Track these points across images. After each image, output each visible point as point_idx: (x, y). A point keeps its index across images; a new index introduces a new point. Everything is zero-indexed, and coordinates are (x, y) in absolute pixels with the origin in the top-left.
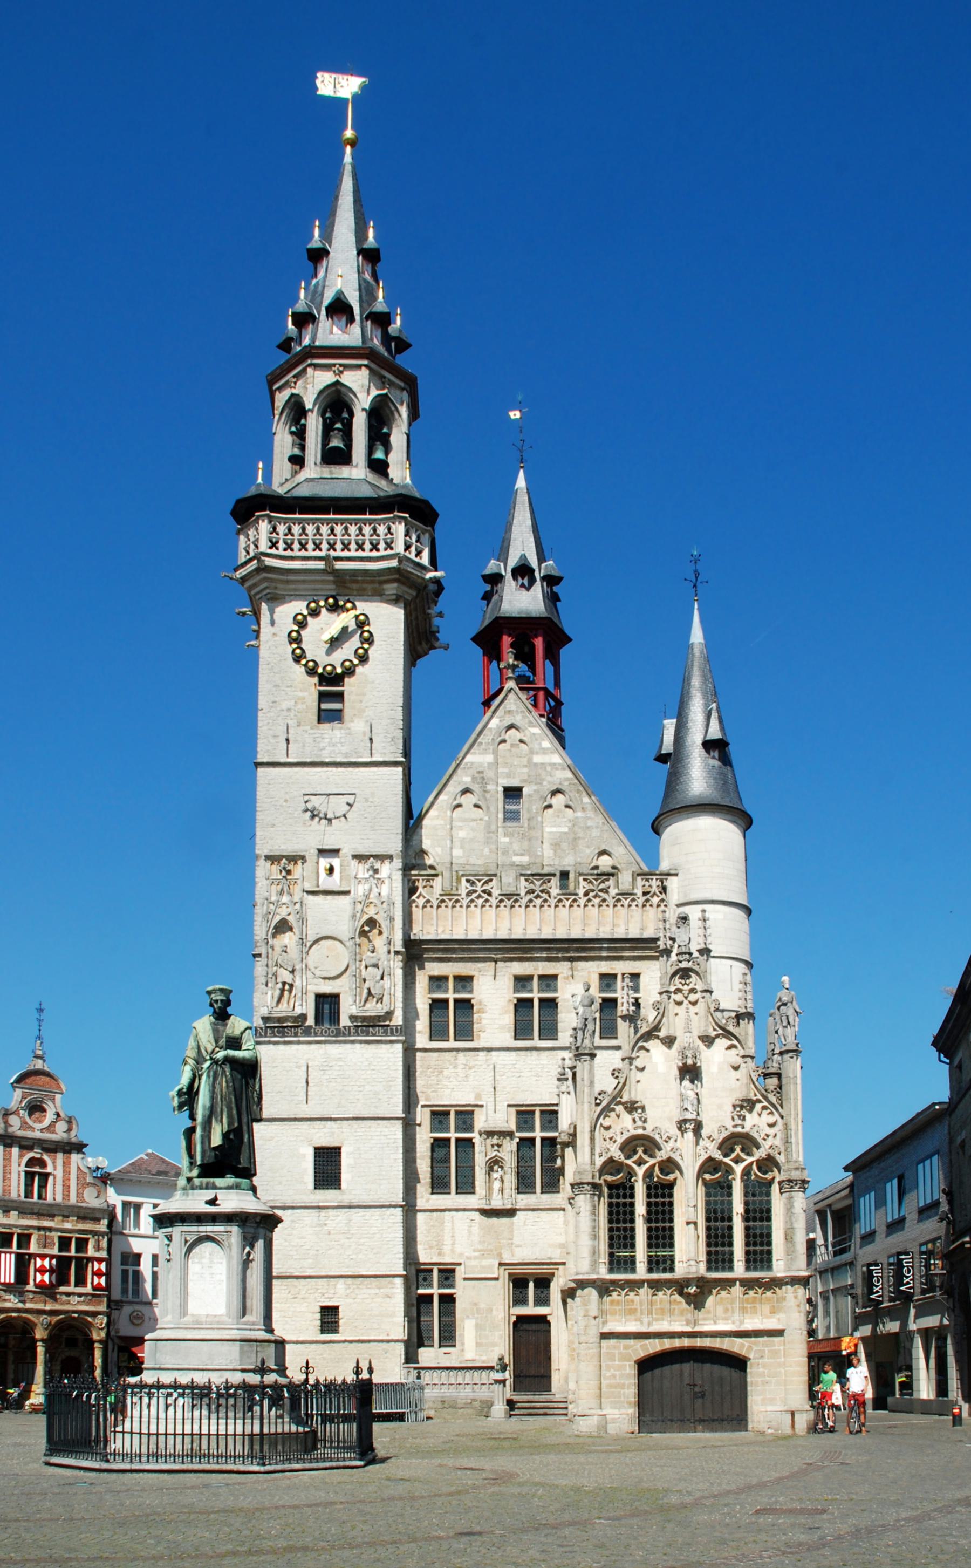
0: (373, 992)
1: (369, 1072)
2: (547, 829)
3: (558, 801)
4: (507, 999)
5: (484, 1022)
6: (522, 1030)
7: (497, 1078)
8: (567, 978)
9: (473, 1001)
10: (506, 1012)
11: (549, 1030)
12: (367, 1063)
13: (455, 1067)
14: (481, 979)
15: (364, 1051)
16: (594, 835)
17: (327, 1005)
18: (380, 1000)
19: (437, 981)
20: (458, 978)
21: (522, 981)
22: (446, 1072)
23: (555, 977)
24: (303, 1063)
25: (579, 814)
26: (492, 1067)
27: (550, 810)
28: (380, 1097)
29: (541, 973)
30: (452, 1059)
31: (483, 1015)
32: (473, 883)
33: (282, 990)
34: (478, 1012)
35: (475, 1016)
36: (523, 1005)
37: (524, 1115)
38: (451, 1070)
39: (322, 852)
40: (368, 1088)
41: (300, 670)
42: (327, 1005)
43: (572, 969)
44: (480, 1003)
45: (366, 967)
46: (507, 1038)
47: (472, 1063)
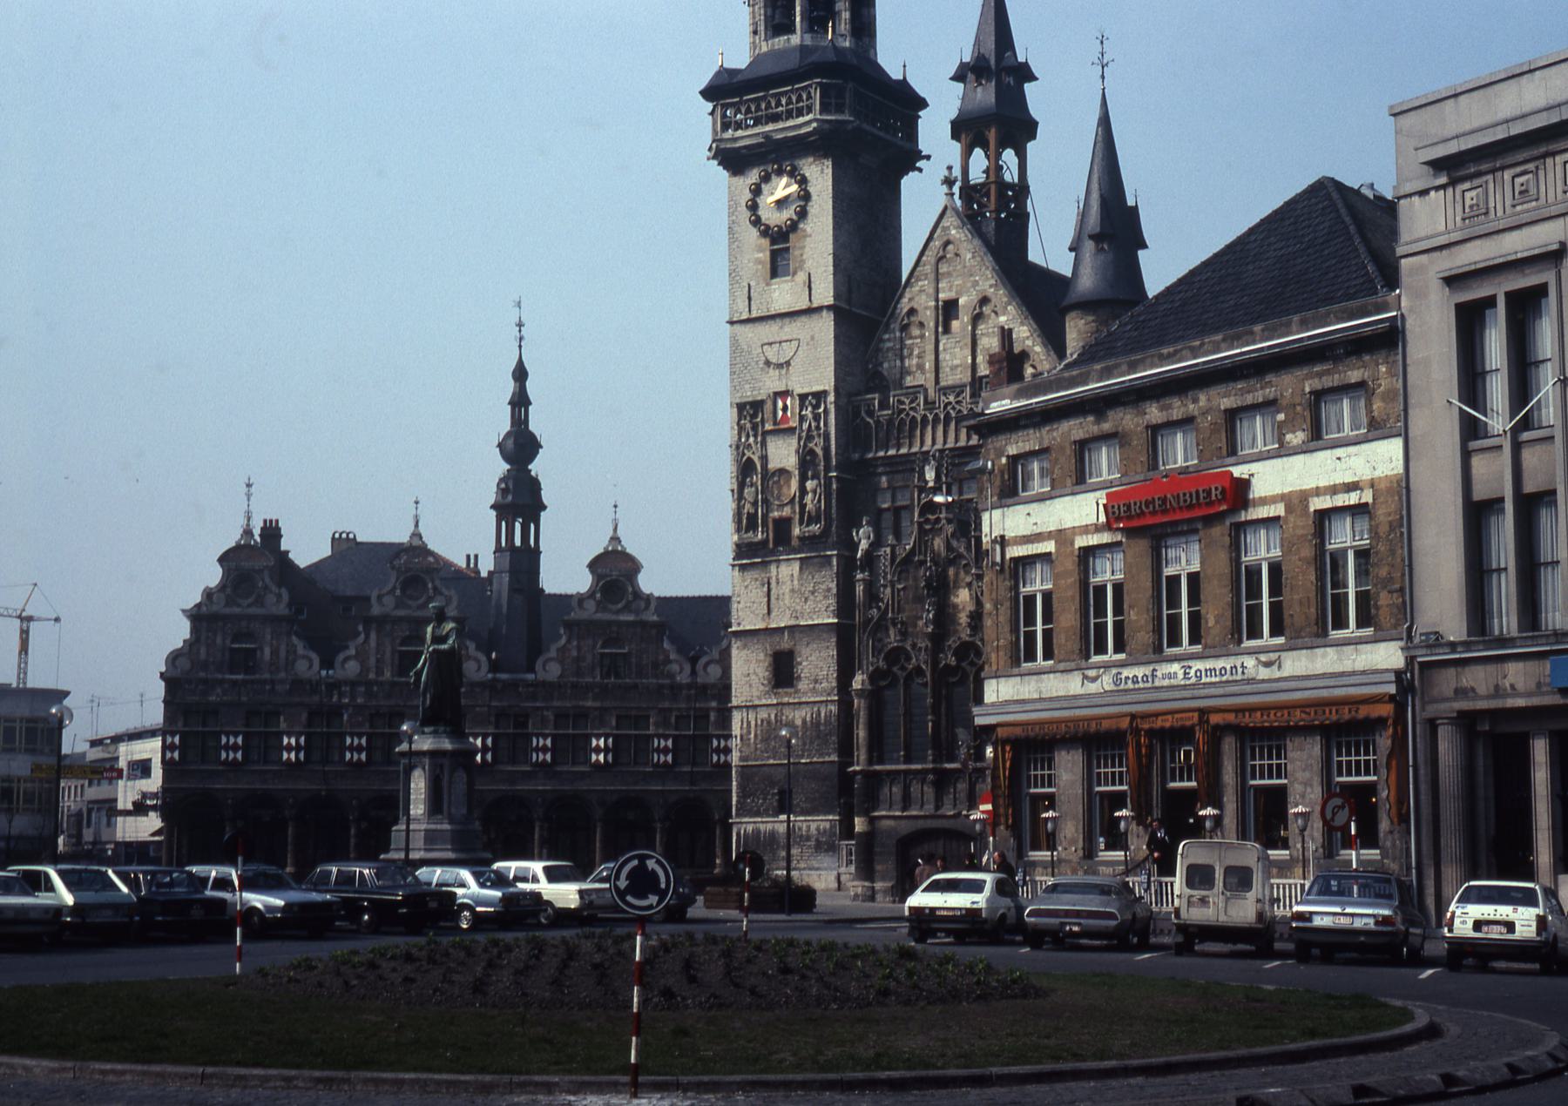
3: (986, 310)
39: (777, 394)
41: (754, 232)
42: (783, 526)
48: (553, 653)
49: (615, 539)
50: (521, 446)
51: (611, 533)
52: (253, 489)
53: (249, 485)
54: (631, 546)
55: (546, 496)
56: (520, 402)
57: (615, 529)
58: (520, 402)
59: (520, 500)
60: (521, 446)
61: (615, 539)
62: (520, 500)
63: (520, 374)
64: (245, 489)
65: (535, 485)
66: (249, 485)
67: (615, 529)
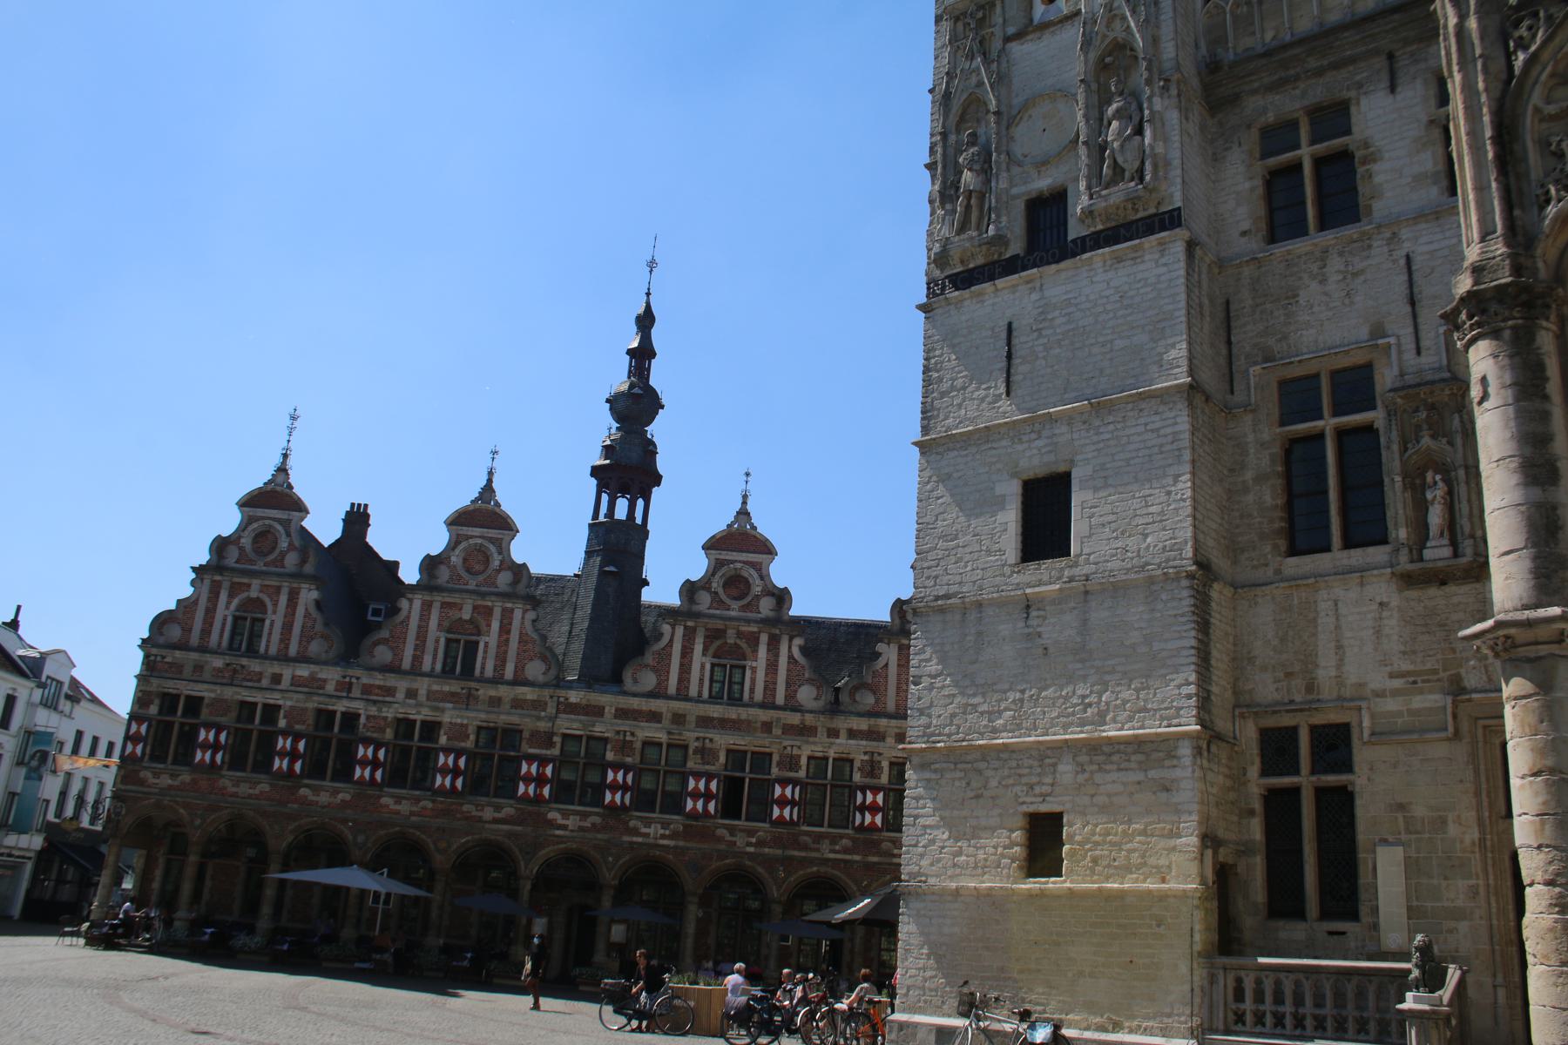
0: (1120, 160)
4: (1424, 119)
5: (1377, 179)
13: (1323, 281)
14: (1364, 102)
15: (1111, 274)
17: (1046, 211)
18: (1140, 175)
19: (1277, 136)
24: (1003, 324)
26: (1403, 262)
31: (1375, 167)
33: (968, 208)
34: (1365, 161)
35: (1361, 170)
38: (1314, 285)
42: (1046, 211)
44: (1366, 145)
48: (649, 658)
49: (743, 513)
50: (636, 406)
51: (738, 506)
52: (296, 424)
53: (294, 418)
54: (764, 525)
55: (662, 464)
56: (642, 356)
57: (744, 503)
58: (642, 356)
59: (629, 469)
60: (636, 406)
61: (743, 513)
62: (629, 469)
63: (646, 321)
64: (289, 422)
65: (650, 449)
66: (294, 418)
67: (744, 503)
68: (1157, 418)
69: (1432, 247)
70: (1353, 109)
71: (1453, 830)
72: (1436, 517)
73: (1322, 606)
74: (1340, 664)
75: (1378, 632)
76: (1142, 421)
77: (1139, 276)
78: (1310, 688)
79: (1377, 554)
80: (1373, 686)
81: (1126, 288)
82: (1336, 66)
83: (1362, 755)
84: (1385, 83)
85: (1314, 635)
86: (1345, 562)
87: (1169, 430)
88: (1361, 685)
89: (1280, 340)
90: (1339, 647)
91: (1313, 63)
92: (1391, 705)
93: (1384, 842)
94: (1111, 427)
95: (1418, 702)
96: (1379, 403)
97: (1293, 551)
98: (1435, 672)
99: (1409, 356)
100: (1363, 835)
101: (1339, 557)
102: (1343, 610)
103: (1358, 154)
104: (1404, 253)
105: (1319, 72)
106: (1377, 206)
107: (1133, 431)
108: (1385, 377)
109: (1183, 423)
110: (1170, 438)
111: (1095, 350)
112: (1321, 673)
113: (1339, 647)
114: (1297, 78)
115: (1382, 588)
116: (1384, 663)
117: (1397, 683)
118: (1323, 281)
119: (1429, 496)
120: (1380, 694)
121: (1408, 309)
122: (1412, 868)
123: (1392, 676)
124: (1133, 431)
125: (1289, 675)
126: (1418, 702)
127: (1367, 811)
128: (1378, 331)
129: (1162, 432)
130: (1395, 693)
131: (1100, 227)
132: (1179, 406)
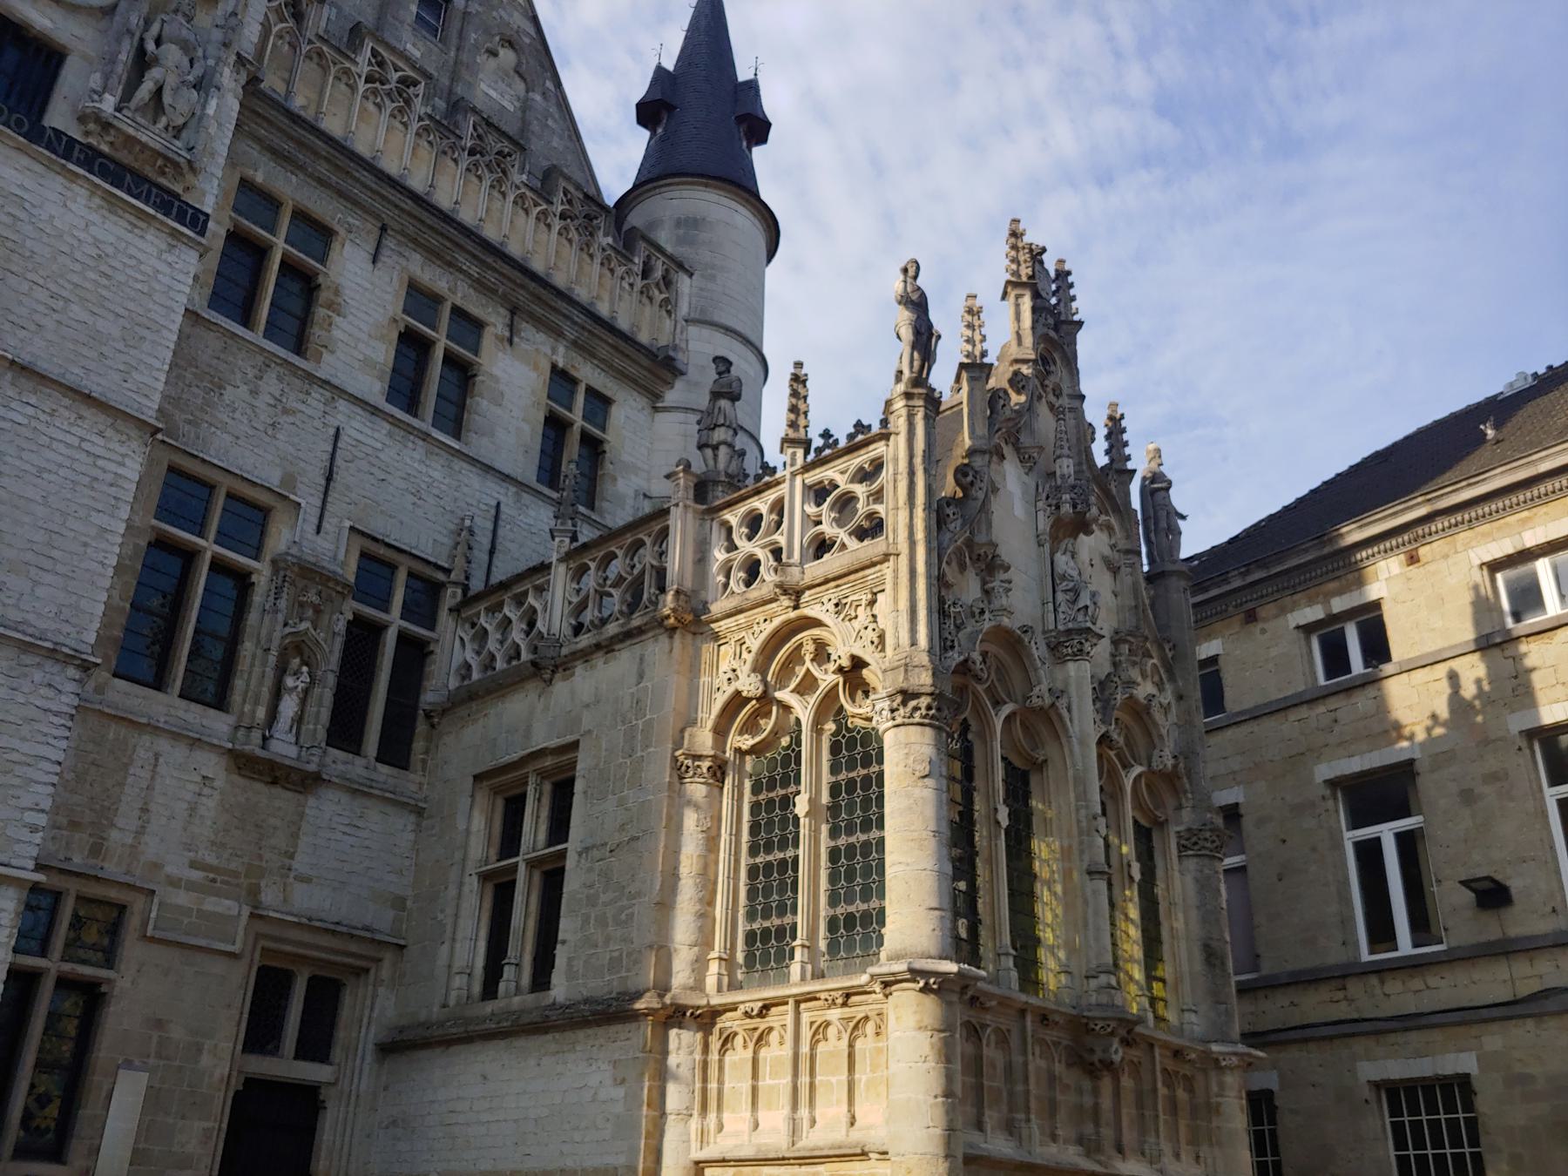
0: (167, 98)
1: (92, 275)
2: (483, 86)
3: (507, 56)
5: (336, 333)
6: (405, 389)
7: (339, 461)
8: (500, 339)
9: (321, 279)
10: (382, 338)
11: (454, 418)
12: (94, 252)
13: (254, 392)
15: (94, 217)
16: (555, 144)
20: (300, 216)
21: (420, 298)
22: (229, 393)
23: (478, 325)
25: (538, 98)
26: (332, 431)
27: (492, 63)
28: (104, 349)
29: (459, 303)
30: (251, 373)
31: (337, 319)
32: (381, 64)
34: (330, 306)
35: (320, 312)
36: (413, 345)
37: (378, 562)
40: (76, 311)
43: (511, 327)
44: (337, 292)
45: (158, 42)
46: (374, 388)
47: (292, 402)
68: (100, 441)
69: (360, 437)
70: (336, 246)
71: (206, 1060)
72: (289, 706)
73: (141, 752)
74: (140, 832)
75: (193, 809)
76: (80, 432)
77: (132, 251)
78: (96, 850)
79: (218, 724)
80: (169, 869)
81: (110, 250)
82: (341, 194)
83: (132, 950)
84: (371, 248)
85: (121, 784)
86: (181, 713)
87: (112, 467)
88: (157, 866)
89: (190, 422)
90: (145, 810)
91: (323, 169)
92: (182, 898)
93: (129, 1065)
94: (30, 411)
95: (212, 904)
96: (268, 556)
97: (115, 675)
98: (236, 874)
99: (311, 528)
100: (105, 1048)
101: (166, 706)
102: (162, 769)
103: (324, 295)
104: (336, 423)
105: (322, 182)
106: (326, 356)
107: (61, 436)
108: (280, 538)
109: (132, 470)
110: (109, 478)
111: (41, 295)
112: (114, 835)
113: (145, 810)
114: (301, 168)
115: (212, 765)
116: (188, 847)
117: (197, 875)
118: (254, 392)
119: (290, 682)
120: (174, 883)
121: (323, 482)
122: (154, 1099)
123: (194, 865)
124: (61, 436)
125: (74, 825)
126: (212, 904)
127: (120, 1020)
128: (289, 480)
129: (100, 462)
130: (191, 886)
131: (105, 148)
132: (134, 445)
